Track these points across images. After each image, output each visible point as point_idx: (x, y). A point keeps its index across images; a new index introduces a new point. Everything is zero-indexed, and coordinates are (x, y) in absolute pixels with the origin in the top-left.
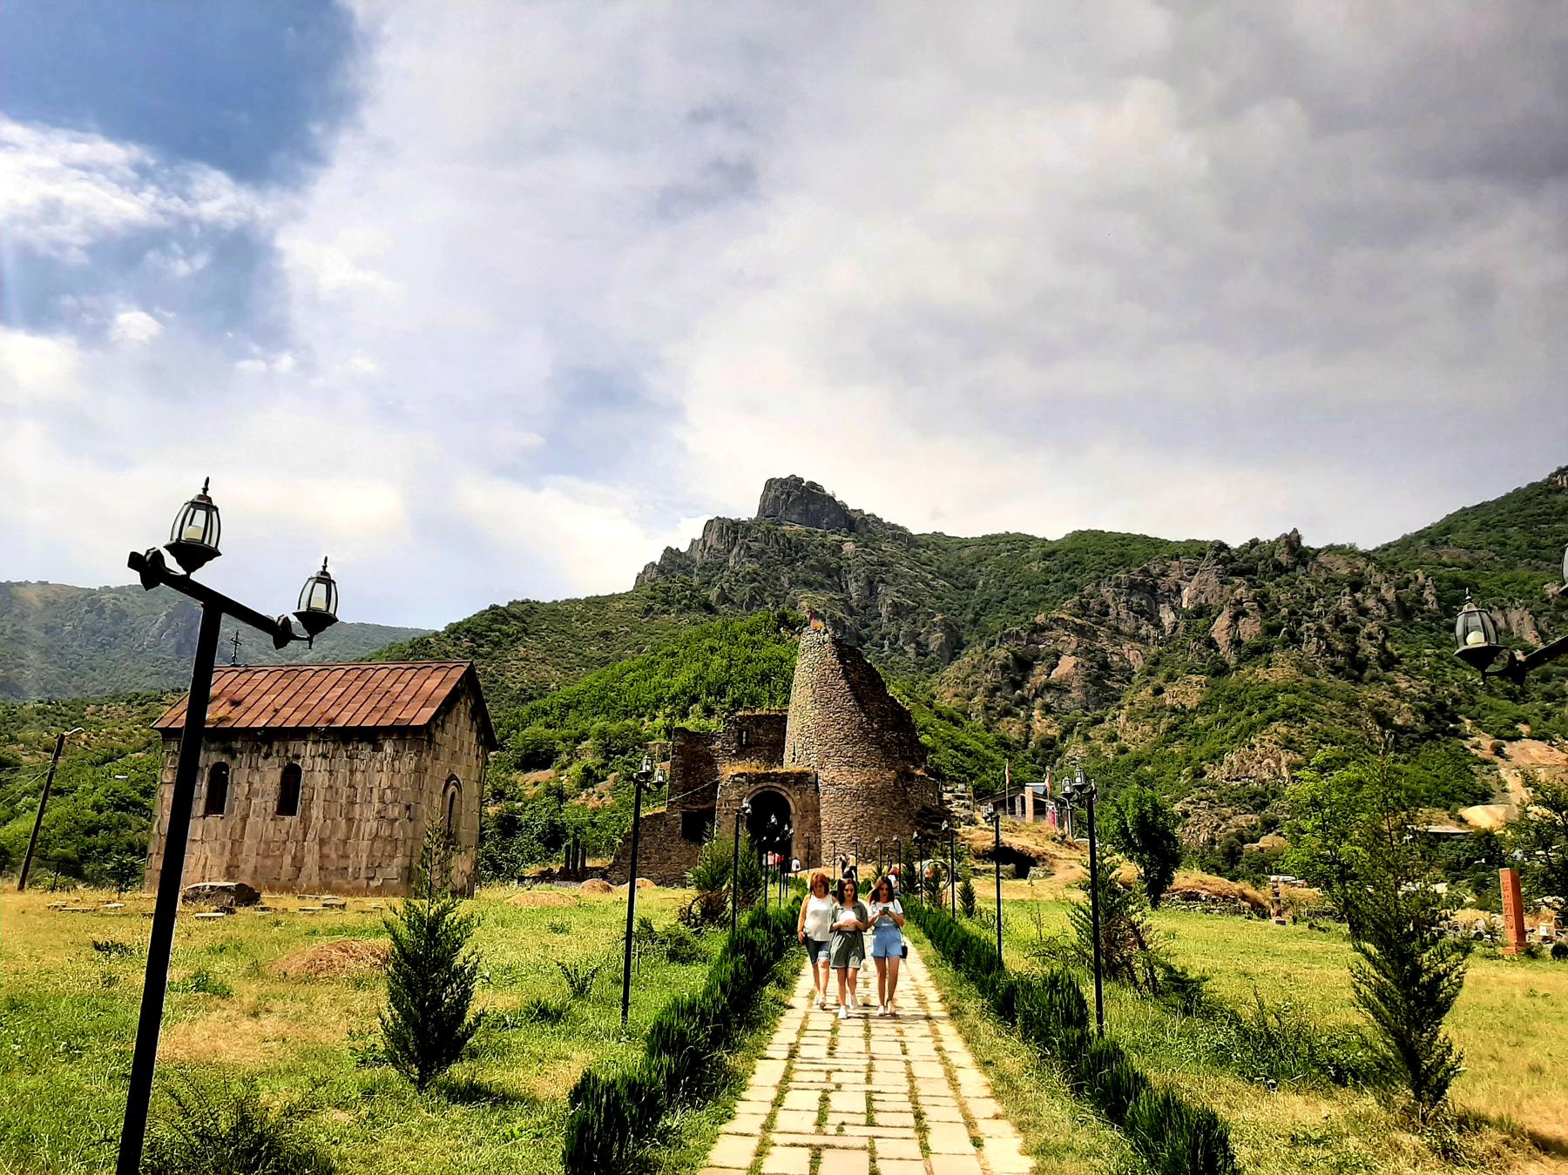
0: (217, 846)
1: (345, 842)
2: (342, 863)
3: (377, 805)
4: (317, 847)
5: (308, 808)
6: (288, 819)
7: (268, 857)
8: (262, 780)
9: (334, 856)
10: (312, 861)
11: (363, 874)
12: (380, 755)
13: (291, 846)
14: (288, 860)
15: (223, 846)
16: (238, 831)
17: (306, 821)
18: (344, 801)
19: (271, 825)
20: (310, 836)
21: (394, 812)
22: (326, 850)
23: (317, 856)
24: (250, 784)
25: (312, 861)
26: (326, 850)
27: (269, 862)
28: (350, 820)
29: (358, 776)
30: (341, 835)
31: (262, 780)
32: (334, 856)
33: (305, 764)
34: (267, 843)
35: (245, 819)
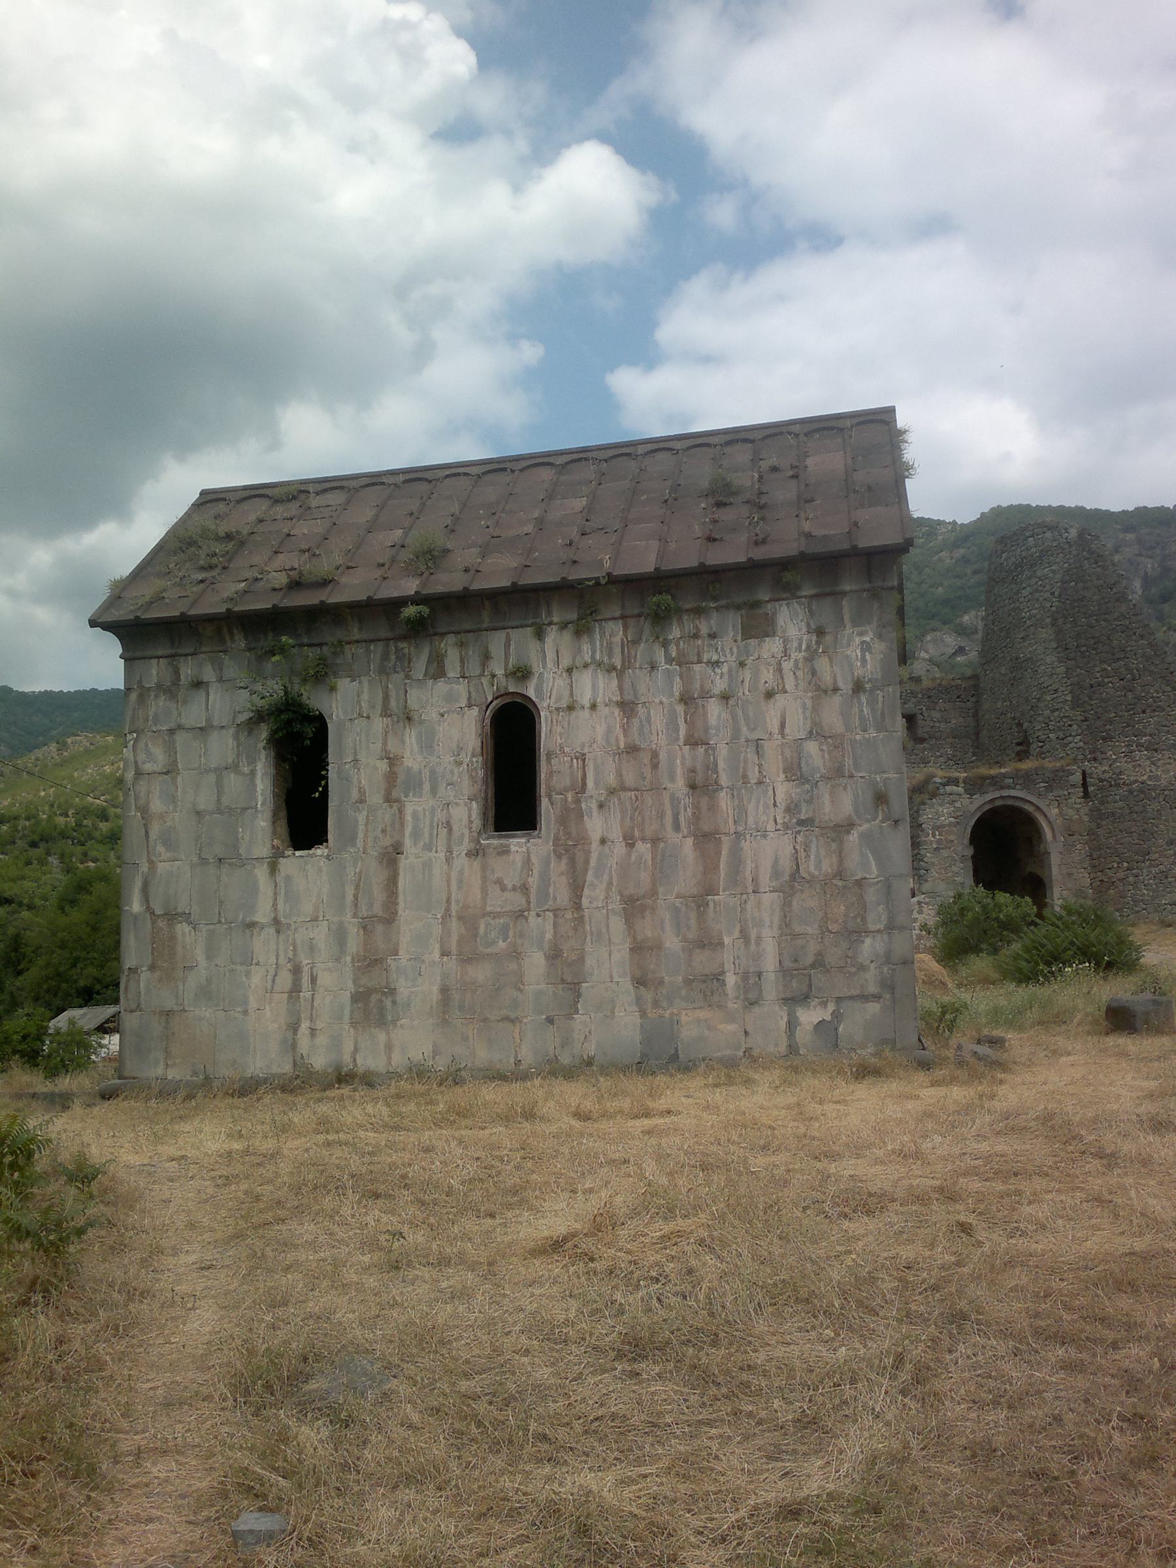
0: (320, 934)
1: (701, 899)
2: (702, 962)
3: (783, 790)
4: (617, 925)
5: (572, 815)
6: (517, 843)
7: (467, 960)
8: (428, 745)
9: (672, 943)
10: (607, 964)
11: (771, 987)
12: (772, 646)
13: (541, 926)
14: (535, 963)
15: (340, 935)
16: (379, 896)
17: (572, 849)
18: (679, 785)
19: (470, 870)
20: (594, 894)
21: (840, 803)
22: (646, 929)
23: (621, 952)
24: (392, 760)
25: (607, 964)
26: (646, 929)
27: (480, 973)
28: (706, 839)
29: (714, 711)
30: (686, 879)
31: (428, 745)
32: (672, 943)
33: (547, 690)
34: (469, 920)
35: (392, 856)
